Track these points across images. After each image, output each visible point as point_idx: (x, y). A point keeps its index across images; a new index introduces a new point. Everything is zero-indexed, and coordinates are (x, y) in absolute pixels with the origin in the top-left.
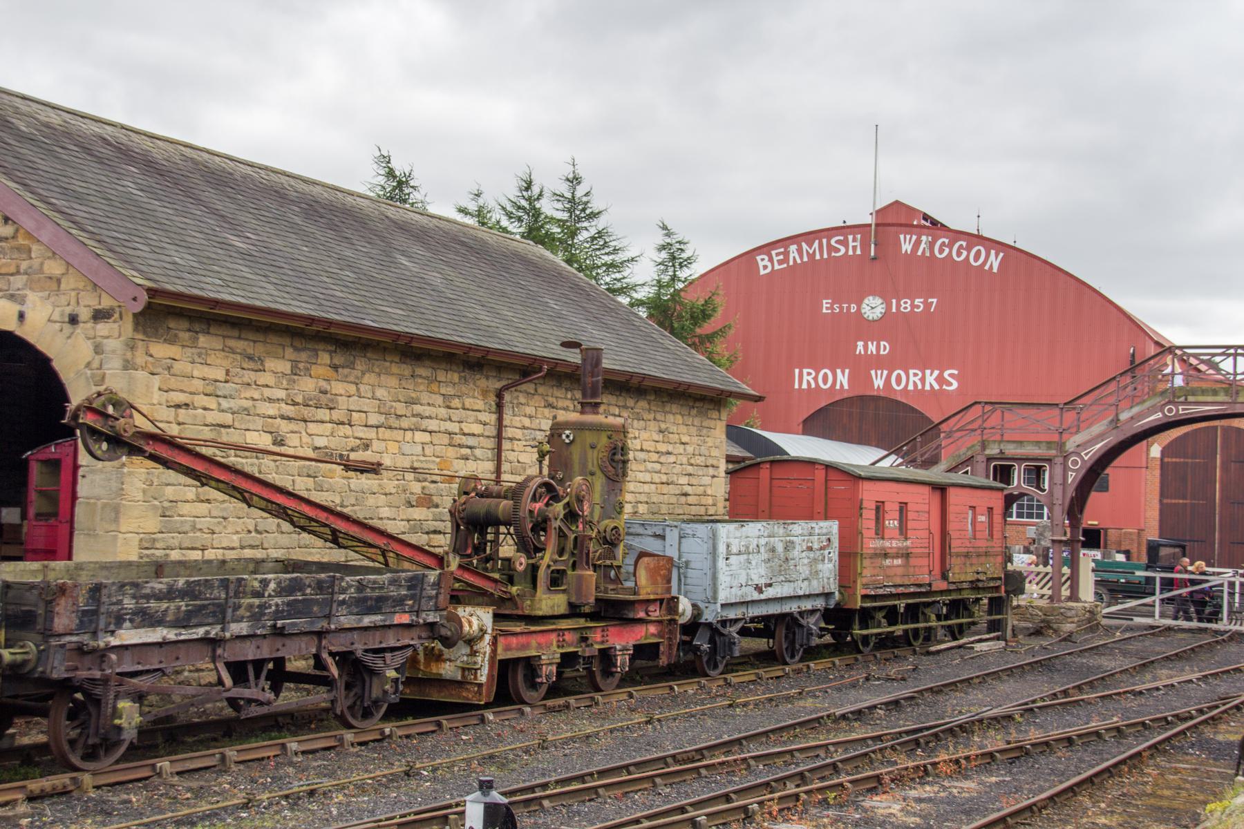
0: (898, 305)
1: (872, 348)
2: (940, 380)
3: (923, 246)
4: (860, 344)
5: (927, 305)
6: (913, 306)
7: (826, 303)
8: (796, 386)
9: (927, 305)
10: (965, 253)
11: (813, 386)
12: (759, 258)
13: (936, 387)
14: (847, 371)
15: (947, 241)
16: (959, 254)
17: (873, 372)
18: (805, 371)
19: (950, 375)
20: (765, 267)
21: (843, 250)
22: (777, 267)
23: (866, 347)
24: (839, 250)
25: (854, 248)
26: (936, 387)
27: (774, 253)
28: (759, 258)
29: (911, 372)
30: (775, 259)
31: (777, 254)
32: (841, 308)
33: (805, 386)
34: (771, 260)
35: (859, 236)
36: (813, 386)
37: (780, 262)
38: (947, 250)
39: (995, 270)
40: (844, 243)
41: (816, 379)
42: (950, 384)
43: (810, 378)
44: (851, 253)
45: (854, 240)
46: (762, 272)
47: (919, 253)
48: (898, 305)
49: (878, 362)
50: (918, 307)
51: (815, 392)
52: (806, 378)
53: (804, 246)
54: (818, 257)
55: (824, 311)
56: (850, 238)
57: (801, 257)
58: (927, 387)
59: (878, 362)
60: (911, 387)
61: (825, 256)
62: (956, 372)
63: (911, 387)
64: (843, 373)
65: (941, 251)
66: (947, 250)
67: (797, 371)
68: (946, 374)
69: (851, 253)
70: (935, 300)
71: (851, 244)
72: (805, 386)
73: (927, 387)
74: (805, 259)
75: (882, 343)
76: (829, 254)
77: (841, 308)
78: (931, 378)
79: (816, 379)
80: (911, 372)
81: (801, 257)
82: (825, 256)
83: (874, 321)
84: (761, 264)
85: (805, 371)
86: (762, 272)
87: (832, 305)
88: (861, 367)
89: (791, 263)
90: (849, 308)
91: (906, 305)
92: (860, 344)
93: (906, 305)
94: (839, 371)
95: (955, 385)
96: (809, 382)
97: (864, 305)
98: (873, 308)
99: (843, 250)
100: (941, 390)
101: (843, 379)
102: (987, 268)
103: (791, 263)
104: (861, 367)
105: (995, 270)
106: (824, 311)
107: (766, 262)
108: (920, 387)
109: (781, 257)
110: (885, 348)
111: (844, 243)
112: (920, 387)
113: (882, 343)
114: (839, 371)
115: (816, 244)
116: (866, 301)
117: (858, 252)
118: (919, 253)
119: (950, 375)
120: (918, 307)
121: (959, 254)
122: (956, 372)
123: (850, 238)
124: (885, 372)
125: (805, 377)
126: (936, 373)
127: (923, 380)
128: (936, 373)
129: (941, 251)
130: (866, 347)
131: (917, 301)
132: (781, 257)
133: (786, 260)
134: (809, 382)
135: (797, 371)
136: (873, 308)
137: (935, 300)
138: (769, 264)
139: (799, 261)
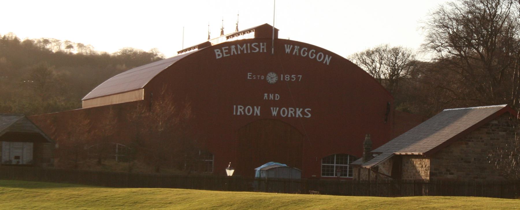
0: (284, 78)
1: (271, 97)
2: (303, 113)
3: (295, 50)
4: (266, 94)
5: (298, 79)
6: (291, 78)
7: (249, 75)
8: (235, 114)
9: (298, 79)
10: (314, 55)
11: (243, 114)
12: (216, 50)
13: (301, 116)
14: (259, 107)
15: (306, 49)
16: (312, 56)
17: (272, 108)
18: (239, 107)
19: (308, 111)
20: (219, 55)
21: (258, 50)
22: (225, 55)
23: (268, 96)
24: (255, 50)
25: (263, 49)
26: (301, 116)
27: (223, 48)
28: (216, 50)
29: (290, 109)
30: (224, 51)
31: (225, 49)
32: (257, 77)
33: (239, 114)
34: (222, 52)
35: (265, 44)
36: (243, 114)
37: (226, 53)
38: (306, 54)
39: (328, 64)
40: (259, 46)
41: (244, 110)
42: (308, 115)
43: (241, 110)
44: (261, 51)
45: (263, 45)
46: (218, 57)
47: (294, 53)
48: (284, 78)
49: (275, 104)
50: (293, 79)
51: (243, 117)
52: (240, 110)
53: (239, 46)
54: (245, 52)
55: (249, 78)
56: (261, 44)
57: (237, 51)
58: (297, 116)
59: (275, 104)
60: (289, 116)
61: (249, 52)
62: (310, 110)
63: (289, 116)
64: (258, 108)
65: (304, 53)
66: (306, 54)
67: (235, 106)
68: (306, 110)
69: (261, 51)
70: (301, 76)
71: (262, 47)
72: (239, 114)
73: (297, 116)
74: (239, 53)
75: (276, 95)
76: (251, 50)
77: (257, 77)
78: (299, 112)
79: (244, 110)
80: (290, 109)
81: (237, 51)
82: (249, 52)
83: (272, 84)
84: (217, 53)
85: (239, 107)
86: (218, 57)
87: (252, 75)
88: (266, 106)
89: (232, 54)
90: (260, 77)
91: (287, 78)
92: (266, 94)
93: (287, 78)
94: (255, 107)
95: (310, 115)
96: (240, 112)
97: (268, 77)
98: (272, 78)
99: (258, 50)
100: (303, 117)
101: (257, 111)
102: (324, 62)
103: (232, 54)
104: (266, 106)
105: (328, 64)
106: (249, 78)
107: (219, 53)
108: (294, 116)
109: (227, 51)
110: (278, 97)
111: (259, 46)
112: (294, 116)
113: (276, 95)
114: (255, 107)
115: (245, 46)
116: (269, 75)
117: (265, 51)
118: (294, 53)
119: (308, 111)
120: (293, 79)
121: (312, 56)
122: (310, 110)
123: (261, 44)
124: (278, 109)
125: (239, 110)
126: (301, 110)
127: (295, 113)
128: (301, 110)
129: (304, 53)
130: (268, 96)
131: (293, 76)
132: (227, 51)
133: (229, 52)
134: (240, 112)
135: (235, 106)
136: (272, 78)
137: (301, 76)
138: (221, 54)
139: (236, 53)
